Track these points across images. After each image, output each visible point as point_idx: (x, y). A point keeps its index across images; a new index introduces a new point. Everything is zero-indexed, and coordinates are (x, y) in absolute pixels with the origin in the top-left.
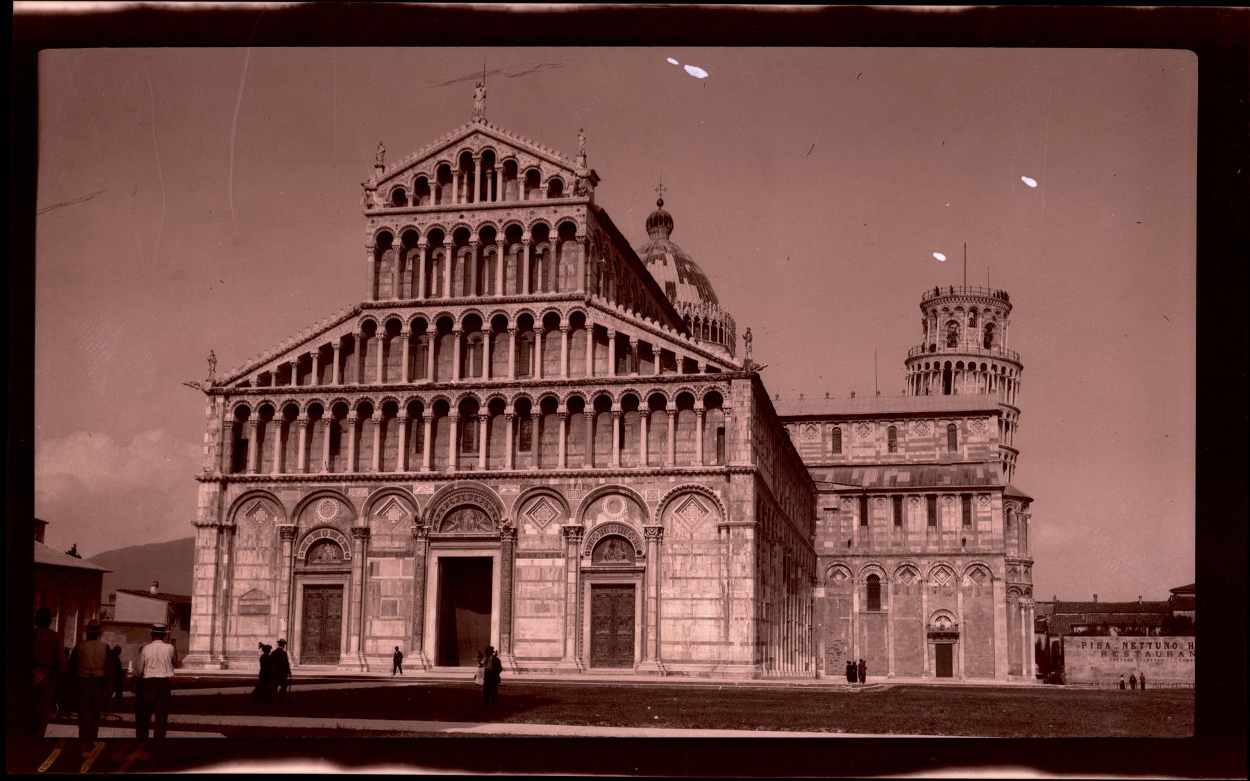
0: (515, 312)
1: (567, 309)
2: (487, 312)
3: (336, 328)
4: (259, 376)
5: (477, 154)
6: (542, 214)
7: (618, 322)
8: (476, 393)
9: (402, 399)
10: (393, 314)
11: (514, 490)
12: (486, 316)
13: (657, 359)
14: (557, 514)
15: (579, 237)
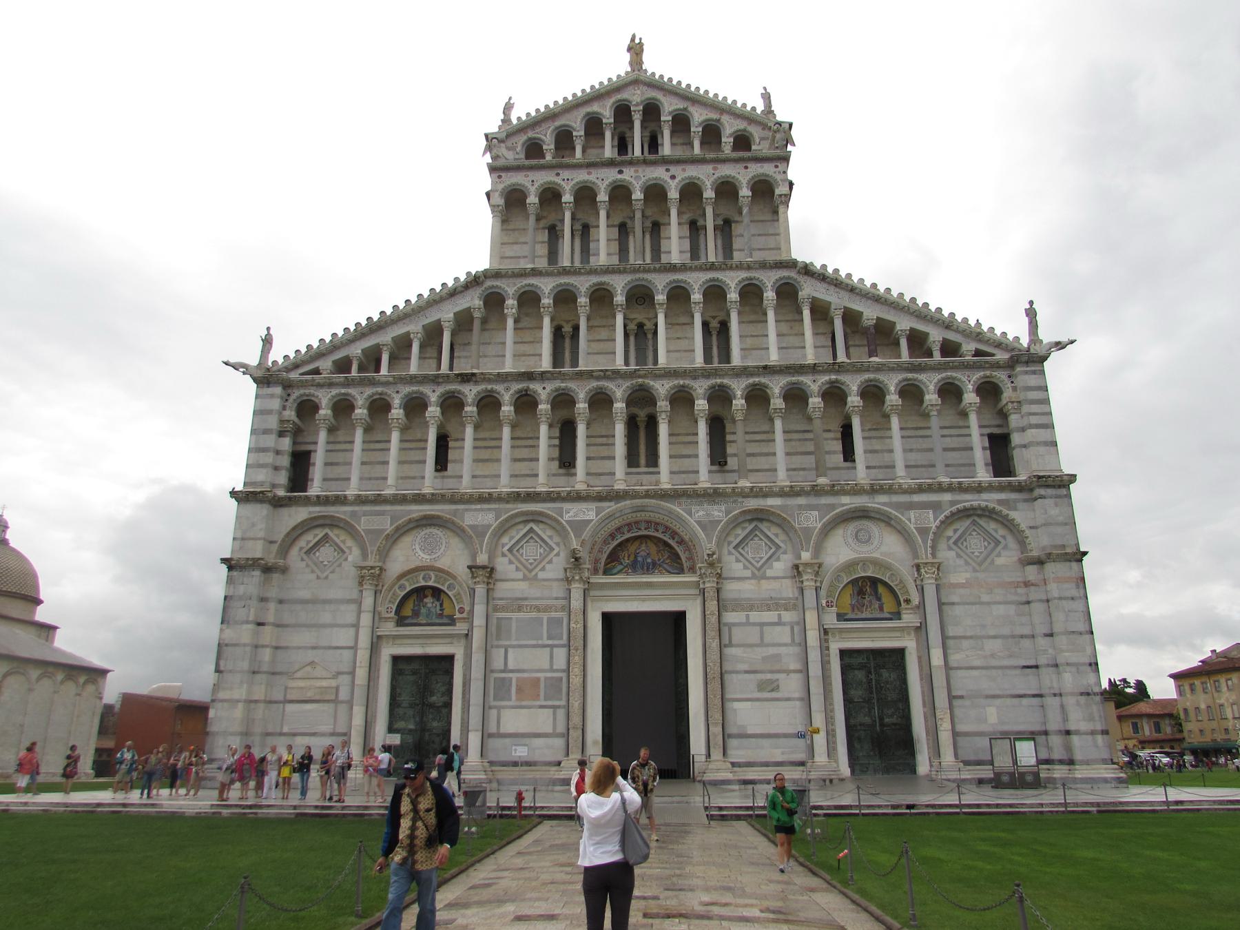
0: (701, 282)
1: (773, 280)
2: (660, 284)
3: (447, 302)
4: (334, 362)
5: (637, 105)
6: (727, 170)
7: (843, 293)
8: (652, 383)
9: (543, 391)
10: (529, 285)
11: (716, 513)
12: (660, 288)
13: (904, 343)
14: (778, 547)
15: (781, 196)
